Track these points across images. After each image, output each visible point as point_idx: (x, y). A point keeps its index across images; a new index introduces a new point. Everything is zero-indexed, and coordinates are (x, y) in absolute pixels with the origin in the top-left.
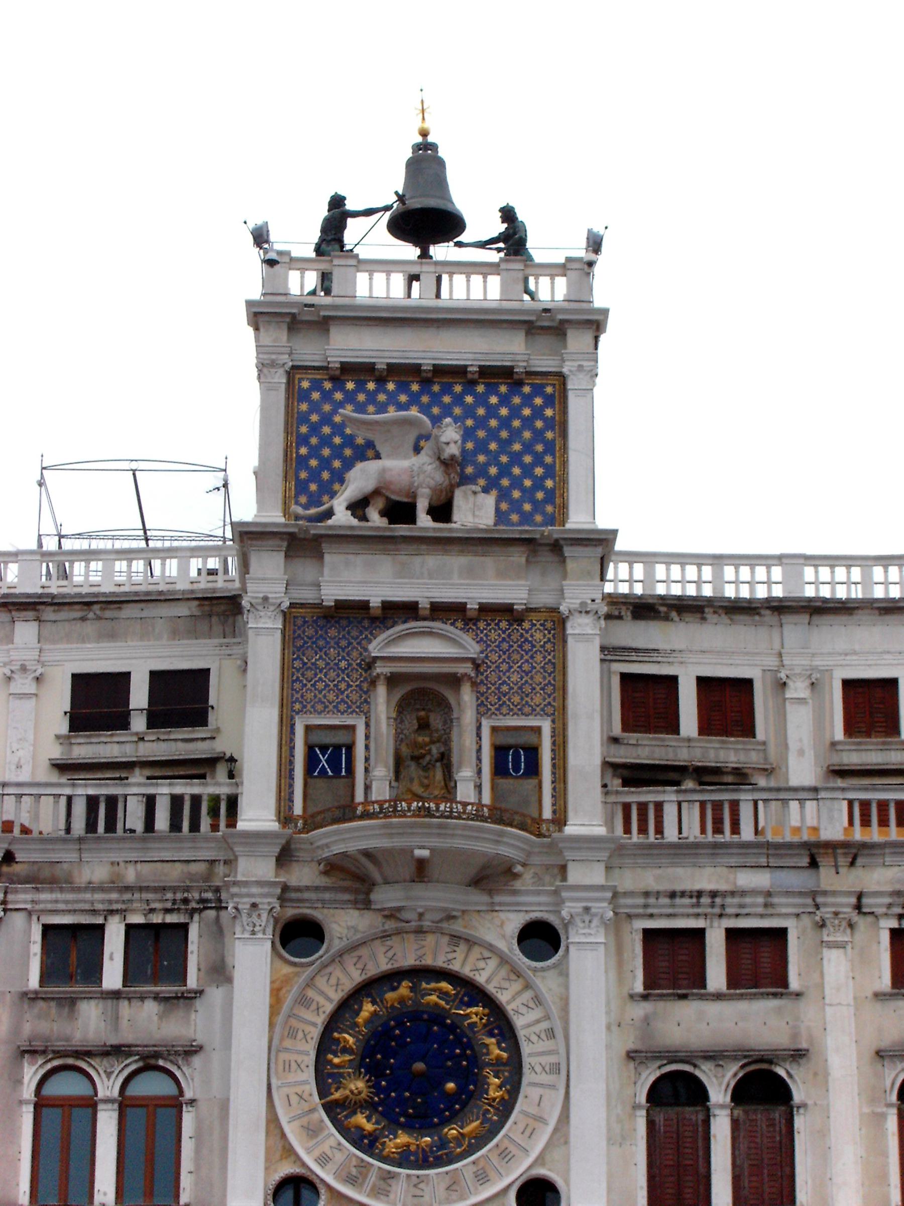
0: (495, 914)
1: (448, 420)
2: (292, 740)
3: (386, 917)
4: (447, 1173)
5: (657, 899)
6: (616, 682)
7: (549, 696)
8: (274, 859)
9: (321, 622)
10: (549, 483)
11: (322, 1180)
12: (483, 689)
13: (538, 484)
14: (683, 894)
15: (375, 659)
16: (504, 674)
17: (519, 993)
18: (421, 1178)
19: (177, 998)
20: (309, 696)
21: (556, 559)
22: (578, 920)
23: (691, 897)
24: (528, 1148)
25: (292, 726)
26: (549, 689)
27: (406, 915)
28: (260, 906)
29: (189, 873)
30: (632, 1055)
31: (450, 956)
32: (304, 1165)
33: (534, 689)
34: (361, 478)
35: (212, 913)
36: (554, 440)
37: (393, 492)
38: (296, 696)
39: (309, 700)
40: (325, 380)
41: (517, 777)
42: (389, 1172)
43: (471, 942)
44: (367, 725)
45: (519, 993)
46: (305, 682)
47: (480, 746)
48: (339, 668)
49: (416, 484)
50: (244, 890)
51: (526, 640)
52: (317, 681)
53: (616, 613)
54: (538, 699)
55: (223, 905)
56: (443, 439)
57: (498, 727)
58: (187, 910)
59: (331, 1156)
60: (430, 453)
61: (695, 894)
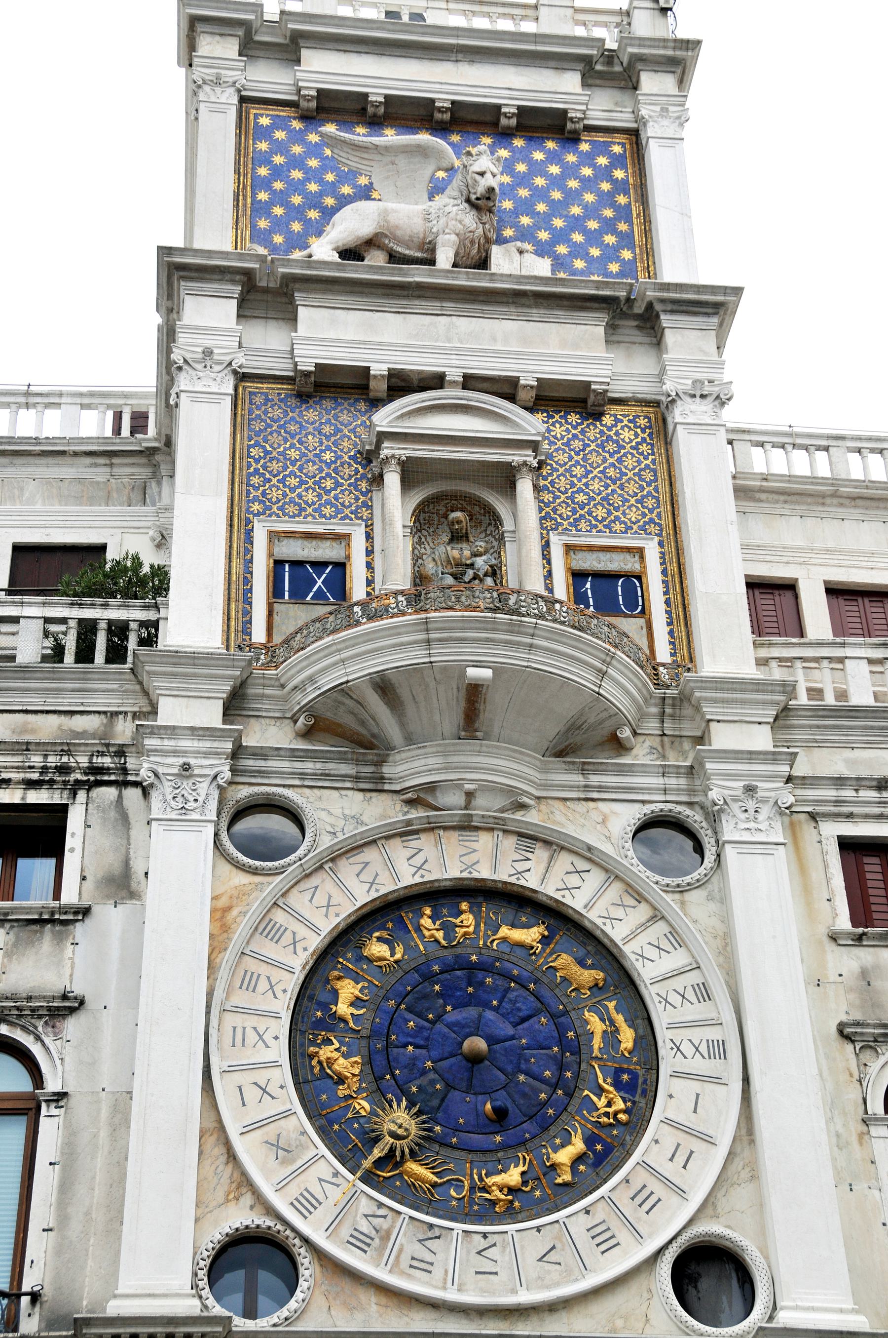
0: (591, 804)
2: (249, 551)
3: (410, 802)
4: (538, 1229)
7: (651, 511)
9: (293, 402)
11: (306, 1241)
15: (382, 437)
16: (580, 480)
17: (644, 926)
18: (491, 1239)
19: (41, 922)
20: (275, 494)
21: (647, 340)
22: (735, 807)
25: (249, 533)
26: (650, 503)
28: (196, 771)
29: (72, 731)
30: (848, 1030)
31: (521, 866)
32: (271, 1211)
33: (627, 501)
35: (110, 792)
37: (399, 241)
38: (253, 493)
39: (274, 500)
40: (295, 118)
44: (369, 537)
45: (644, 926)
46: (268, 476)
48: (321, 461)
49: (434, 230)
50: (168, 744)
51: (609, 438)
52: (289, 476)
54: (633, 515)
55: (130, 778)
56: (476, 168)
57: (575, 546)
58: (65, 783)
59: (321, 1197)
60: (456, 193)
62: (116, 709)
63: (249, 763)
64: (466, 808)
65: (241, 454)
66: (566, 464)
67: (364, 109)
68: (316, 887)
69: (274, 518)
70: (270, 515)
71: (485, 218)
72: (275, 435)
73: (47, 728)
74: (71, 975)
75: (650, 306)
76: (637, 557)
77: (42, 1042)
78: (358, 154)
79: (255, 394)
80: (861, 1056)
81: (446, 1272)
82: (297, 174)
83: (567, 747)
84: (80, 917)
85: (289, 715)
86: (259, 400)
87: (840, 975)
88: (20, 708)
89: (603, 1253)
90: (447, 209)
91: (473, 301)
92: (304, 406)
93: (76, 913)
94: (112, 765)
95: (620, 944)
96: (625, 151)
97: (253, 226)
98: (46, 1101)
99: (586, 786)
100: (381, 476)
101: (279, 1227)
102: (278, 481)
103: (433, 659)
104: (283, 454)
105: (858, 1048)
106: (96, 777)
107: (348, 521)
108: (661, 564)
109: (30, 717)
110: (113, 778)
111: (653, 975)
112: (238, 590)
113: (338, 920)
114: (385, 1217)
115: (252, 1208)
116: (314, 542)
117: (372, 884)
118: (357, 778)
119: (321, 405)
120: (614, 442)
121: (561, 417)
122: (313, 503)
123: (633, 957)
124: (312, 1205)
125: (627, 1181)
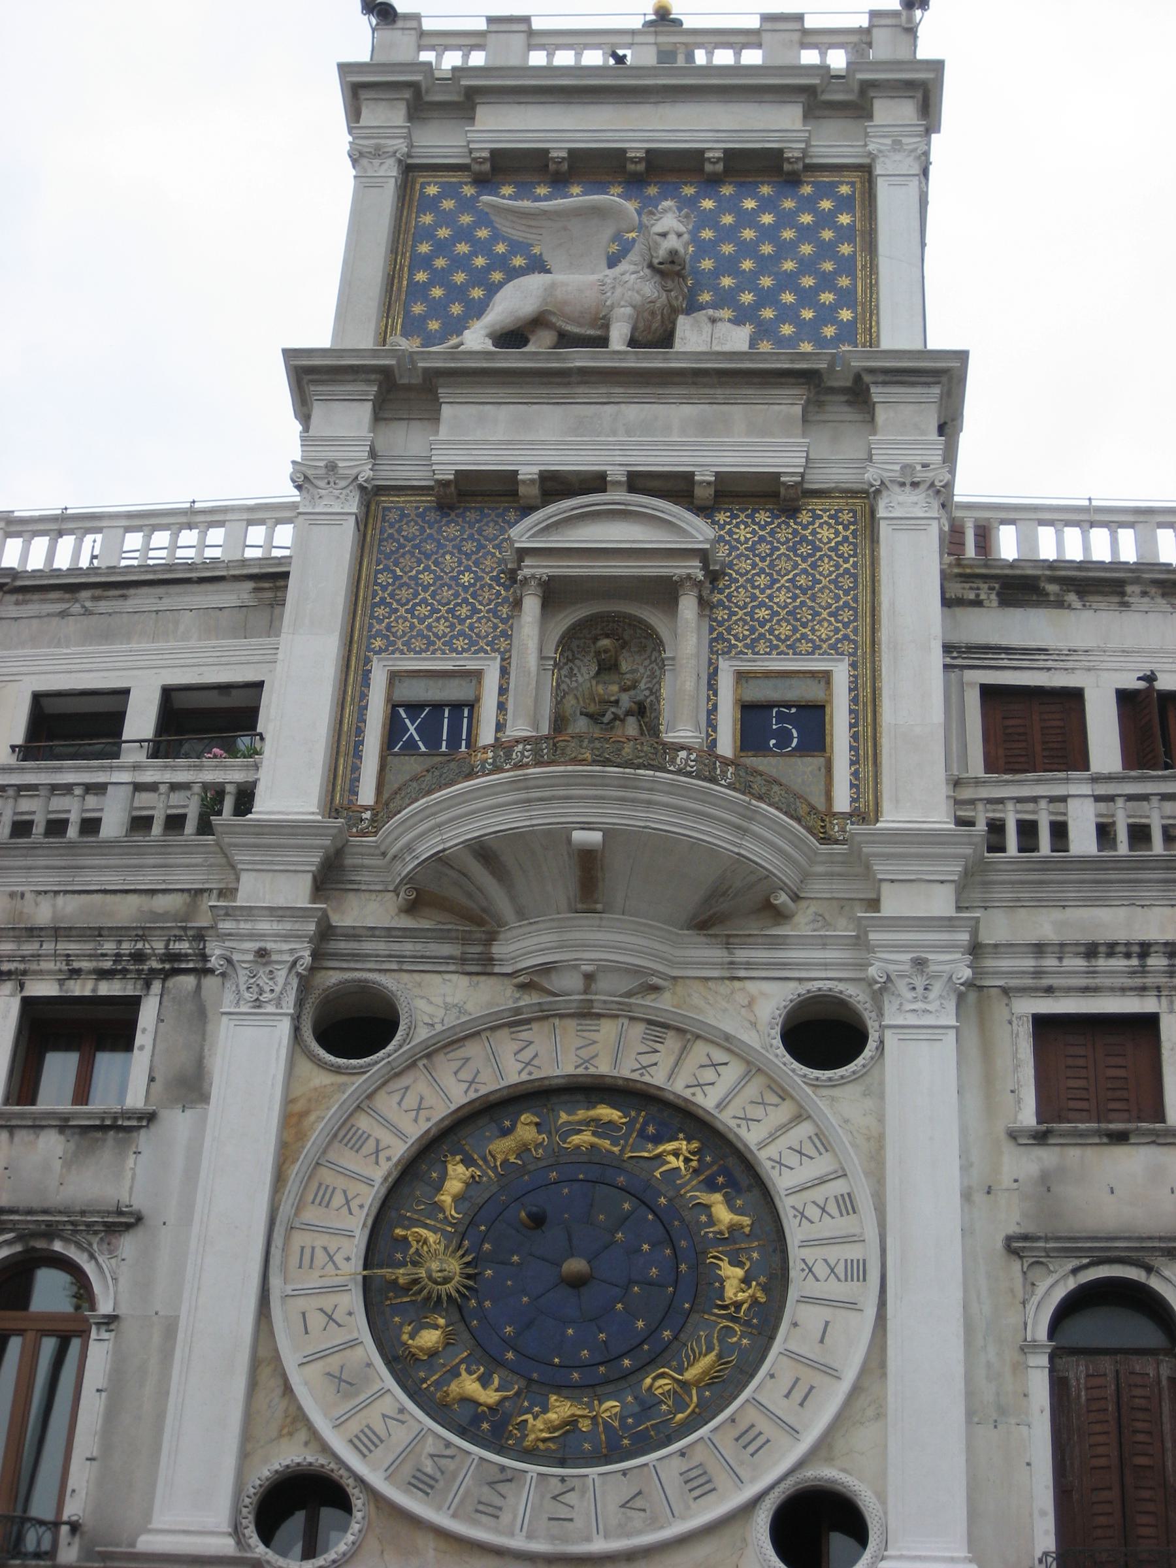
0: (737, 984)
1: (668, 203)
2: (364, 696)
3: (523, 987)
4: (624, 1473)
5: (1060, 959)
6: (973, 699)
7: (846, 625)
8: (309, 878)
9: (432, 516)
10: (845, 315)
11: (361, 1481)
12: (721, 614)
13: (827, 315)
14: (1111, 949)
15: (523, 553)
17: (784, 1128)
18: (570, 1483)
19: (103, 1128)
20: (401, 627)
21: (859, 417)
22: (901, 986)
23: (1128, 955)
24: (797, 1428)
26: (846, 615)
27: (559, 982)
28: (274, 957)
29: (152, 912)
31: (646, 1060)
32: (325, 1448)
33: (819, 614)
34: (515, 300)
35: (189, 981)
36: (853, 256)
37: (570, 319)
40: (466, 184)
41: (782, 755)
42: (503, 1468)
43: (687, 1034)
44: (504, 672)
46: (395, 605)
47: (715, 706)
49: (608, 303)
51: (804, 539)
52: (419, 604)
53: (972, 596)
54: (823, 632)
55: (209, 965)
56: (659, 228)
58: (139, 972)
61: (1136, 949)
62: (201, 886)
63: (343, 946)
64: (585, 992)
65: (367, 581)
66: (747, 572)
67: (547, 166)
68: (407, 1088)
69: (397, 655)
70: (393, 653)
71: (670, 285)
72: (408, 556)
73: (126, 910)
74: (131, 1188)
75: (858, 378)
76: (823, 683)
77: (96, 1260)
78: (524, 222)
79: (389, 509)
80: (1030, 1275)
81: (515, 1517)
82: (463, 248)
83: (711, 917)
84: (144, 1123)
85: (391, 888)
86: (393, 516)
87: (1016, 1181)
88: (98, 888)
89: (696, 1498)
90: (626, 277)
91: (647, 384)
92: (445, 520)
93: (140, 1119)
94: (190, 951)
95: (754, 1148)
96: (854, 192)
97: (407, 312)
98: (97, 1324)
99: (732, 963)
100: (521, 600)
101: (332, 1466)
102: (407, 611)
103: (534, 822)
104: (415, 578)
105: (1026, 1265)
106: (173, 967)
107: (482, 655)
108: (850, 690)
109: (109, 898)
110: (191, 965)
111: (790, 1184)
112: (348, 742)
113: (429, 1124)
114: (452, 1457)
115: (306, 1444)
116: (440, 682)
117: (471, 1083)
118: (463, 960)
119: (464, 518)
120: (809, 543)
121: (747, 517)
122: (445, 635)
123: (768, 1164)
124: (373, 1443)
125: (733, 1421)
